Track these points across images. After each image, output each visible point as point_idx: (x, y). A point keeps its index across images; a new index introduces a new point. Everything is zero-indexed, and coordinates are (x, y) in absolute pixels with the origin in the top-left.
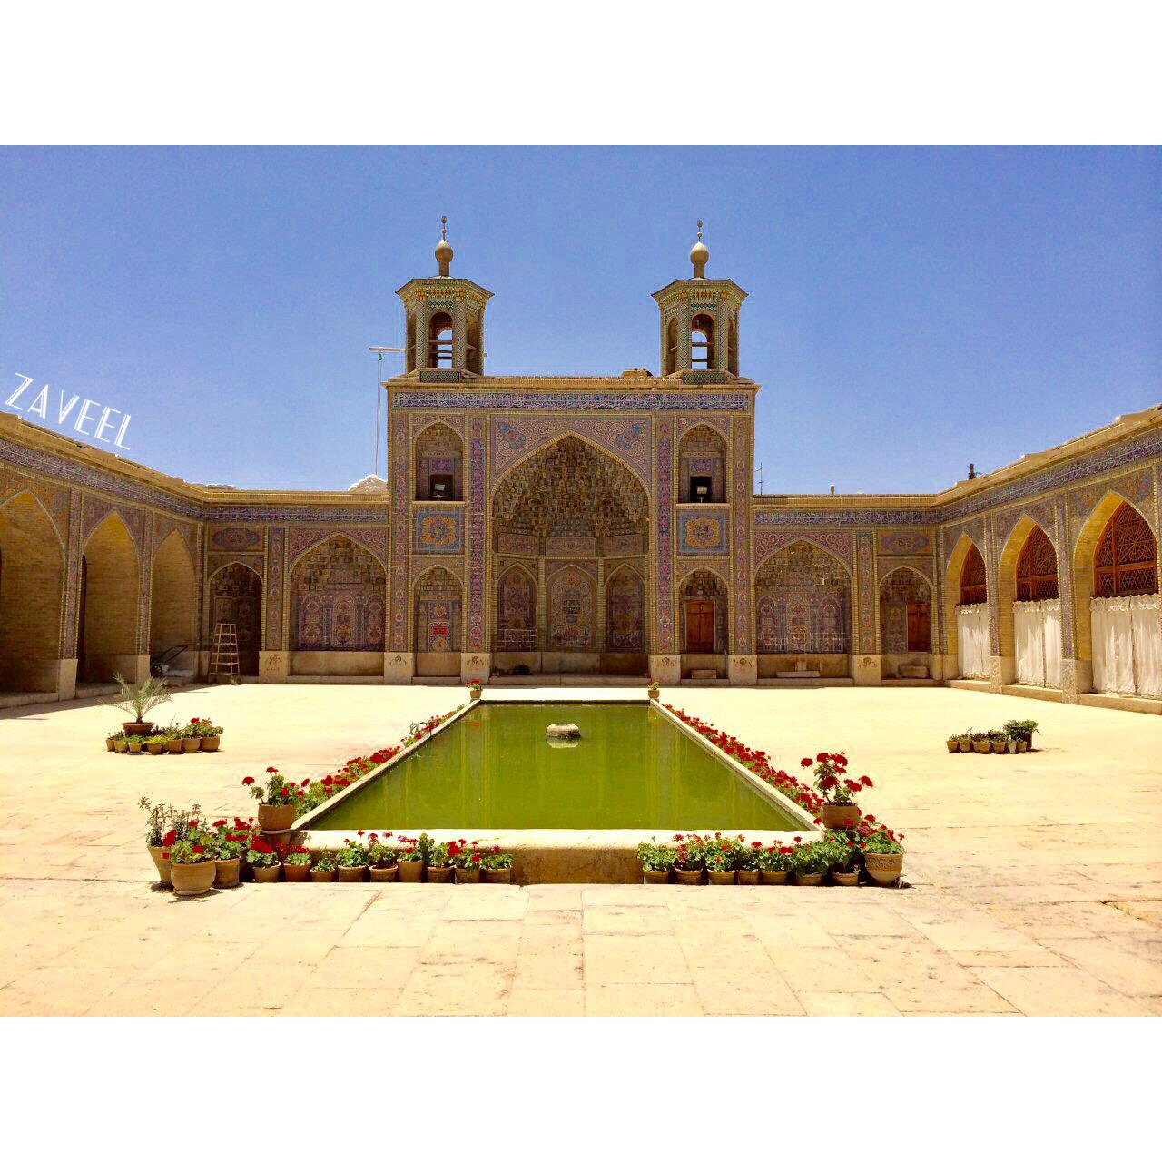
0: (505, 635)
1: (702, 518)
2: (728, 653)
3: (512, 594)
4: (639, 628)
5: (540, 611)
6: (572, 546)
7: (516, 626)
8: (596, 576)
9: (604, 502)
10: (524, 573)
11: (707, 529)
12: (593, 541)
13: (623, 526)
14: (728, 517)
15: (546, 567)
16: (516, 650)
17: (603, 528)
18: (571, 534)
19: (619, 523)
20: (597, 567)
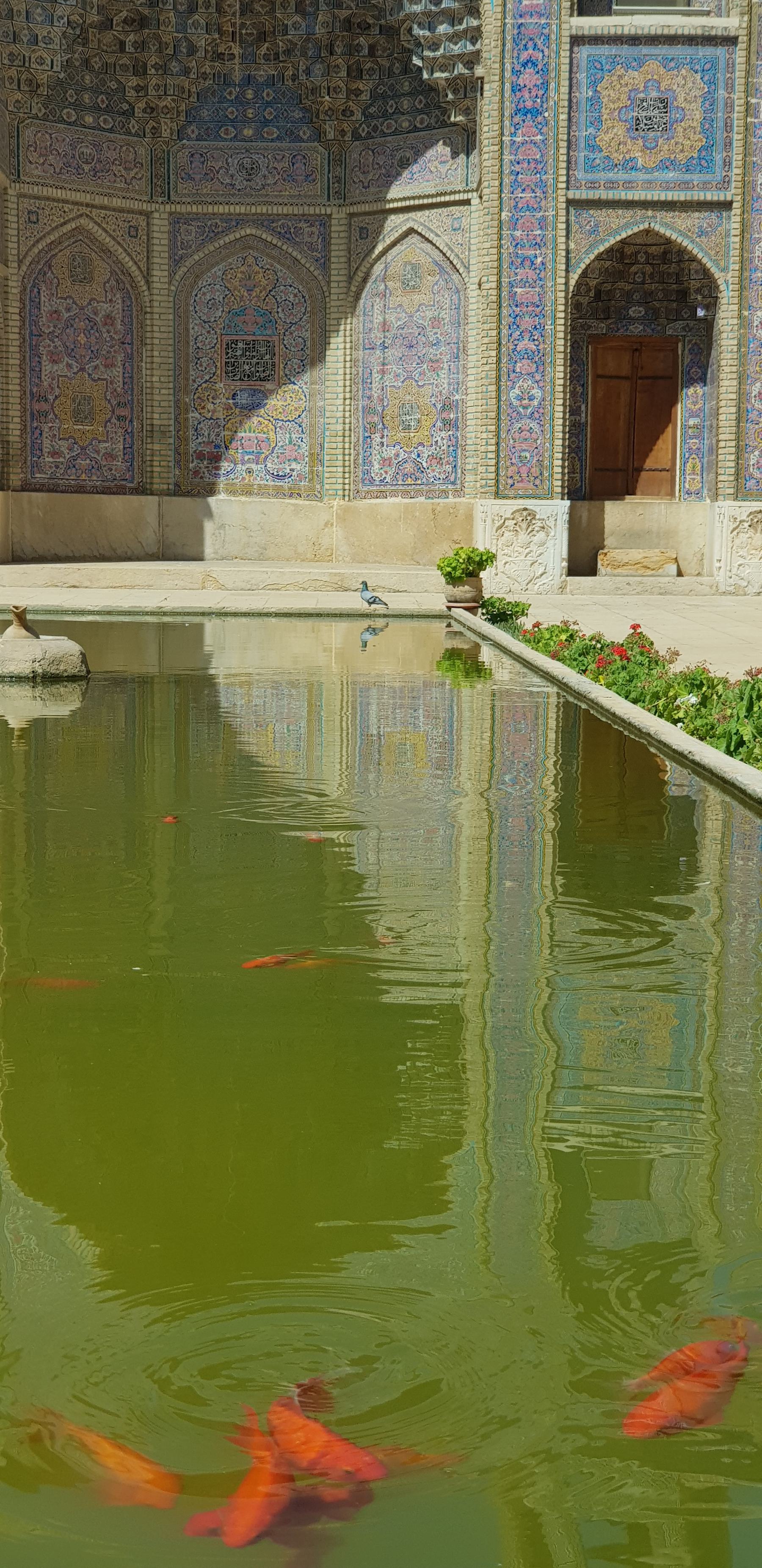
0: (47, 443)
1: (653, 66)
2: (715, 497)
3: (66, 315)
4: (448, 424)
5: (157, 377)
6: (251, 171)
7: (78, 416)
8: (325, 266)
9: (348, 24)
10: (106, 251)
11: (664, 104)
12: (318, 155)
13: (406, 104)
14: (731, 66)
15: (173, 235)
16: (80, 490)
17: (347, 112)
18: (248, 132)
19: (397, 96)
20: (326, 241)
